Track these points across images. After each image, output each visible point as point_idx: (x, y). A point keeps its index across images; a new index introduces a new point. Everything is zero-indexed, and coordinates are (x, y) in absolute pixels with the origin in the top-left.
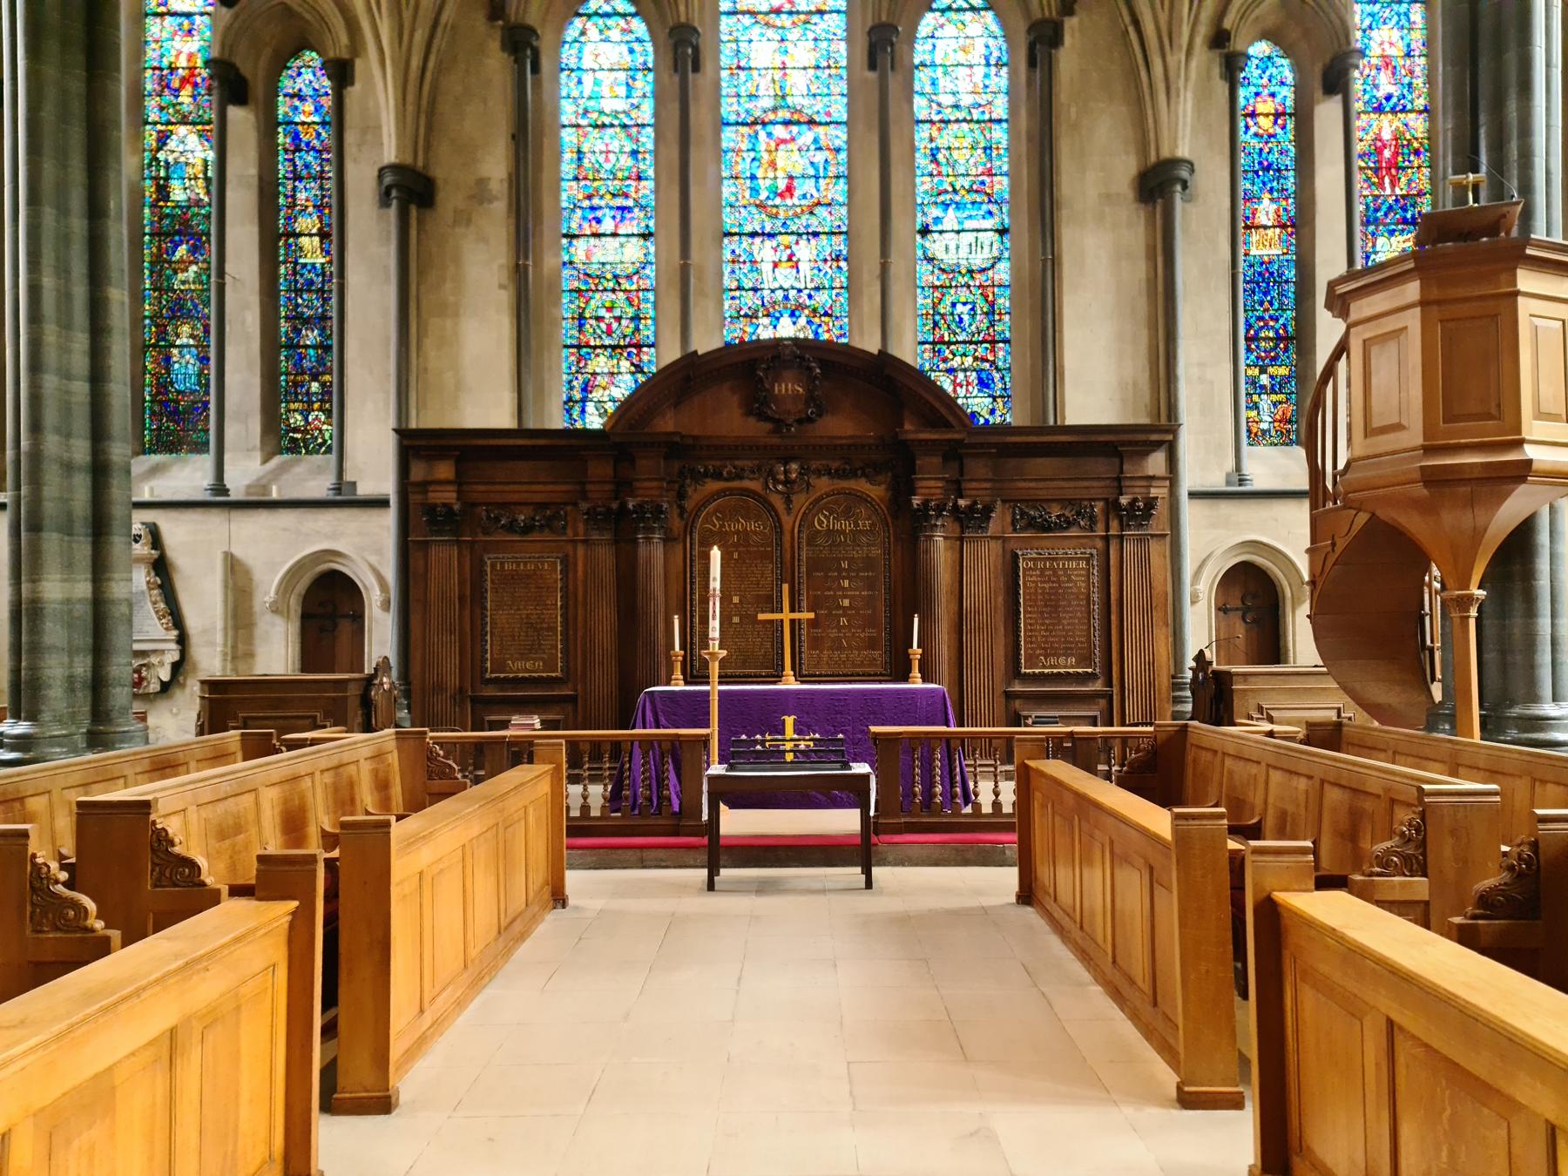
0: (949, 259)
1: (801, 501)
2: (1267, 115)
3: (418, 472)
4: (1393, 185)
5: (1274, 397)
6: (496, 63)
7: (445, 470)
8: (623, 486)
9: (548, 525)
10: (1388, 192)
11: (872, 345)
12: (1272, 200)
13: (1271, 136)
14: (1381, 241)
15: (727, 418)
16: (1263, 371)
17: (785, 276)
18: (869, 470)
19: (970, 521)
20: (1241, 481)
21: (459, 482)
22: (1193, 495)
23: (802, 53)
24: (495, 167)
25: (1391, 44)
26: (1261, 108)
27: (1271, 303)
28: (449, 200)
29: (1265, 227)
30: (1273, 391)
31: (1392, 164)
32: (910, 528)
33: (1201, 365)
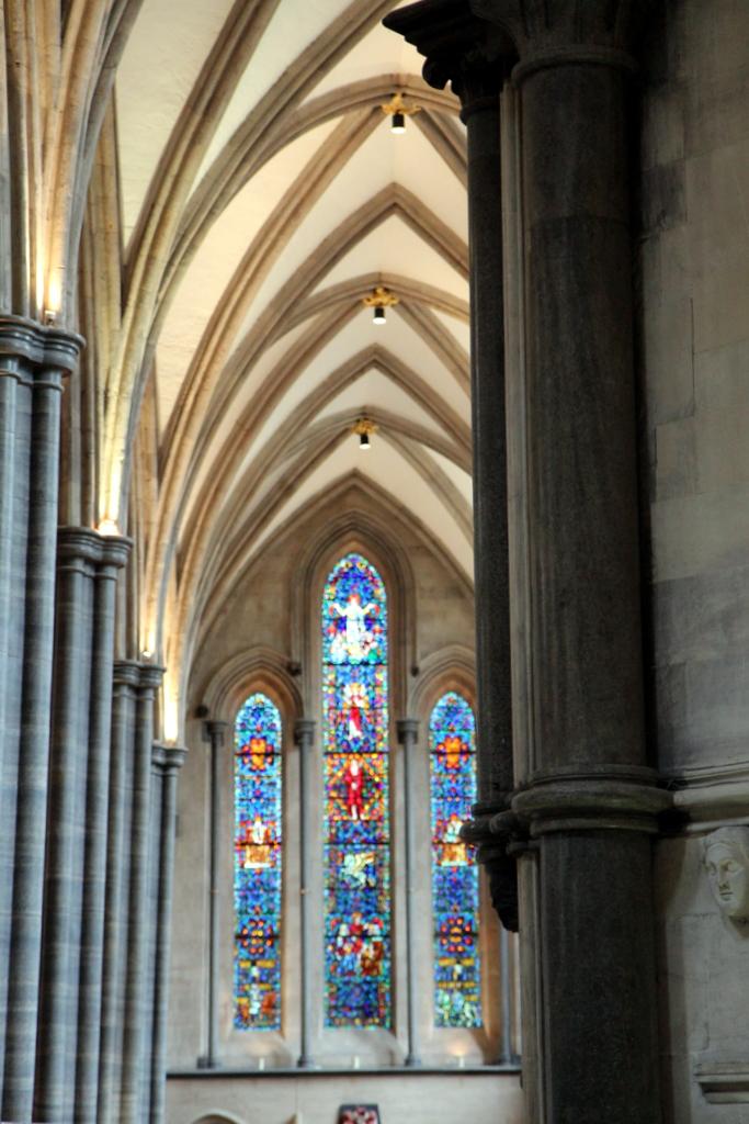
2: (258, 755)
4: (358, 813)
5: (263, 987)
10: (355, 817)
12: (263, 823)
13: (262, 771)
14: (348, 858)
16: (254, 964)
20: (210, 1064)
22: (170, 1077)
25: (360, 698)
26: (256, 748)
27: (261, 907)
29: (257, 845)
30: (261, 982)
31: (358, 795)
33: (181, 968)
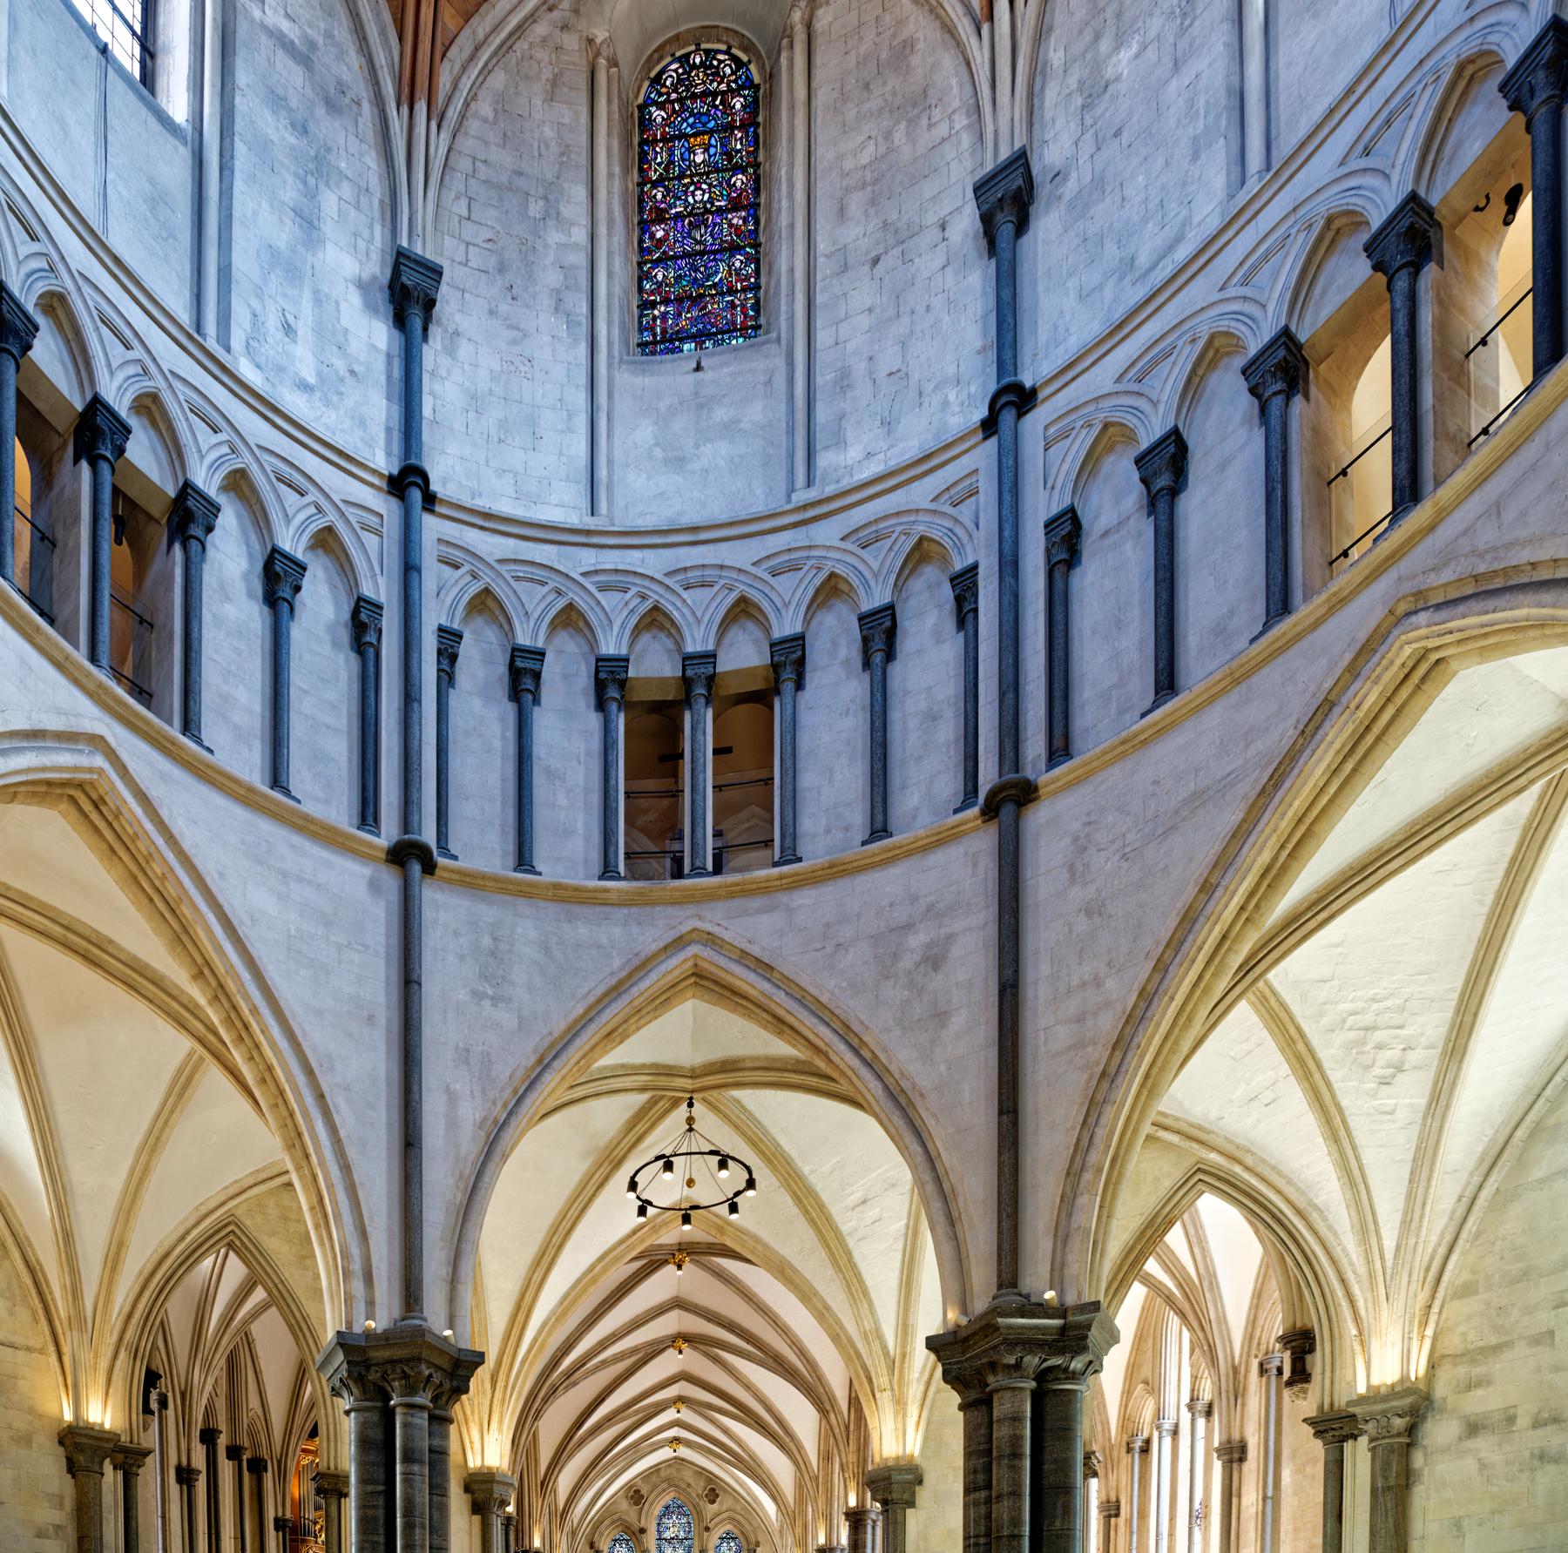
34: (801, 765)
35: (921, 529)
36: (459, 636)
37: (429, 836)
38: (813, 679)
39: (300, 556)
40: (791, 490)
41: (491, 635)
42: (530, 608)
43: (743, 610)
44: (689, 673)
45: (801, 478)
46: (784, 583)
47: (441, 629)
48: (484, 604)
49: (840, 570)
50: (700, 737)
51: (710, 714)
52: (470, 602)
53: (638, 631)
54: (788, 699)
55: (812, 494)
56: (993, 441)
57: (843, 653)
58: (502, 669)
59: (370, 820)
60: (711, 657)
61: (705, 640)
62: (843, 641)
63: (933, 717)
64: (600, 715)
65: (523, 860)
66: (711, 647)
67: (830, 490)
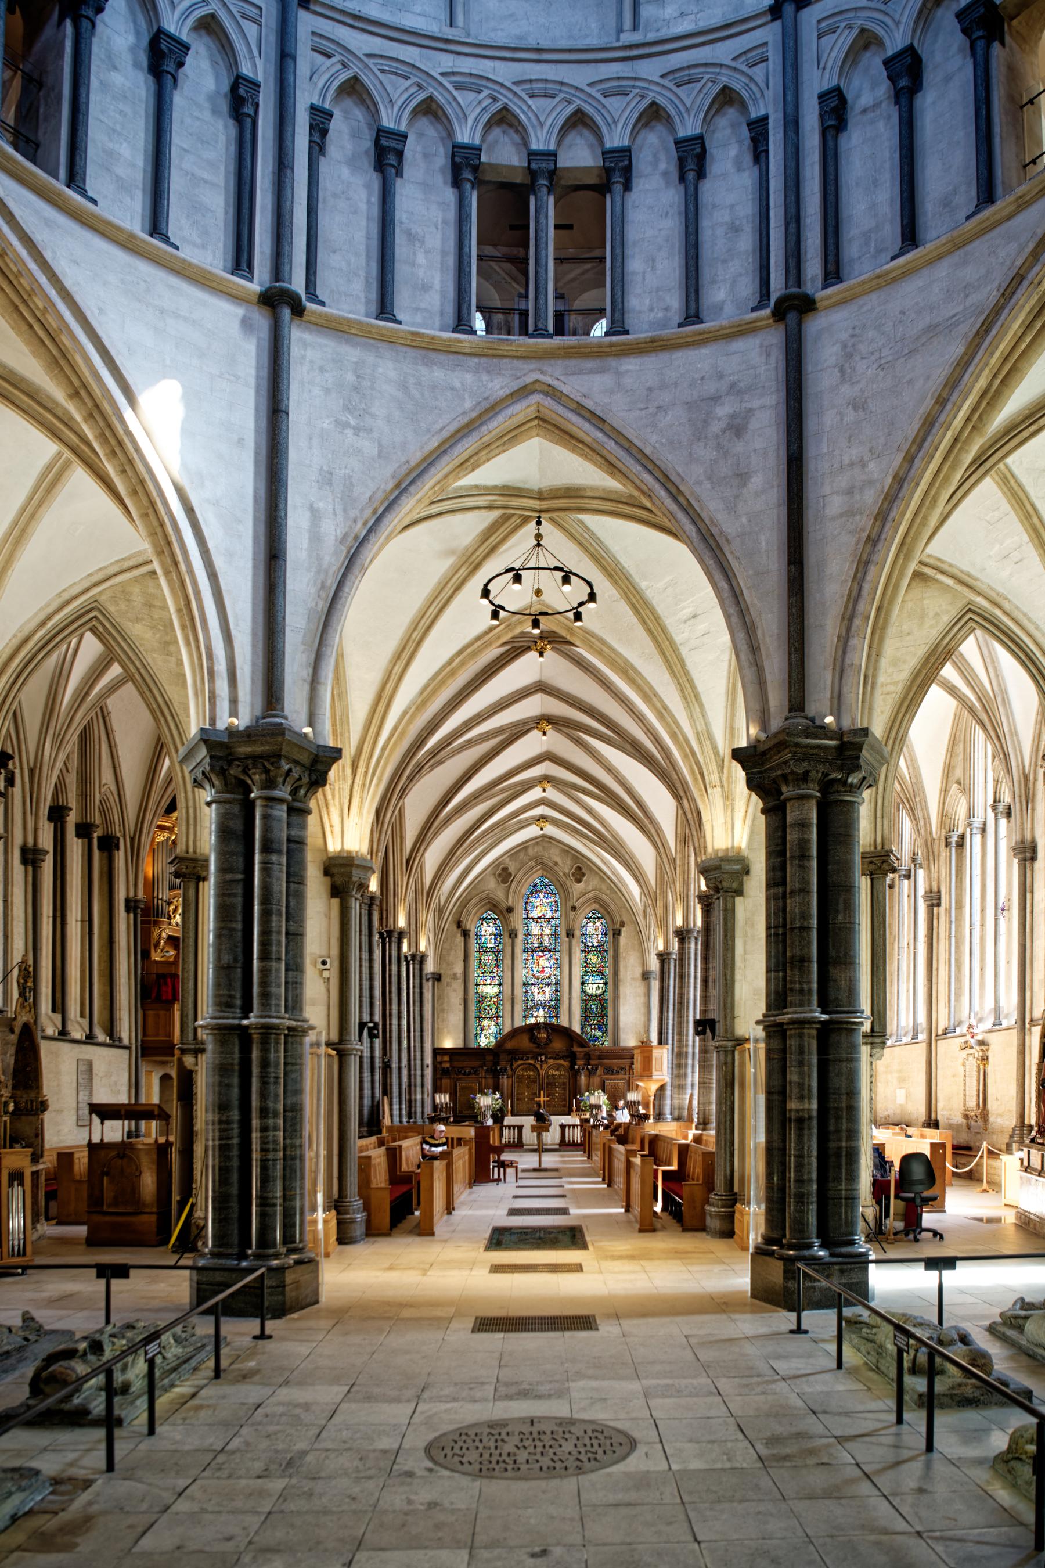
0: (590, 992)
1: (545, 1066)
3: (439, 1058)
6: (460, 939)
7: (446, 1058)
8: (497, 1063)
9: (475, 1073)
11: (565, 1023)
15: (525, 1043)
17: (541, 997)
18: (563, 1058)
19: (591, 1073)
21: (451, 1061)
23: (547, 931)
24: (459, 969)
28: (445, 980)
32: (575, 1074)
34: (629, 252)
35: (724, 80)
36: (330, 115)
37: (298, 284)
38: (640, 185)
39: (184, 37)
40: (620, 30)
41: (359, 114)
42: (394, 96)
43: (579, 120)
44: (534, 166)
45: (628, 24)
46: (614, 104)
47: (313, 107)
48: (353, 89)
49: (660, 100)
50: (543, 220)
51: (551, 200)
52: (340, 86)
53: (489, 125)
54: (618, 198)
55: (637, 37)
56: (778, 24)
57: (663, 166)
58: (368, 144)
59: (244, 266)
60: (553, 155)
61: (547, 140)
62: (662, 156)
63: (735, 229)
64: (456, 191)
65: (384, 308)
66: (552, 147)
67: (651, 36)
